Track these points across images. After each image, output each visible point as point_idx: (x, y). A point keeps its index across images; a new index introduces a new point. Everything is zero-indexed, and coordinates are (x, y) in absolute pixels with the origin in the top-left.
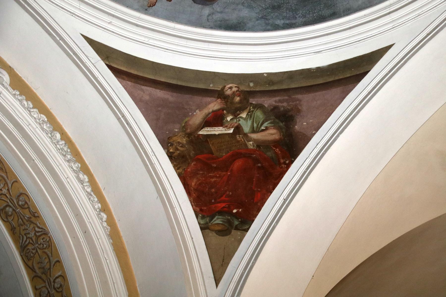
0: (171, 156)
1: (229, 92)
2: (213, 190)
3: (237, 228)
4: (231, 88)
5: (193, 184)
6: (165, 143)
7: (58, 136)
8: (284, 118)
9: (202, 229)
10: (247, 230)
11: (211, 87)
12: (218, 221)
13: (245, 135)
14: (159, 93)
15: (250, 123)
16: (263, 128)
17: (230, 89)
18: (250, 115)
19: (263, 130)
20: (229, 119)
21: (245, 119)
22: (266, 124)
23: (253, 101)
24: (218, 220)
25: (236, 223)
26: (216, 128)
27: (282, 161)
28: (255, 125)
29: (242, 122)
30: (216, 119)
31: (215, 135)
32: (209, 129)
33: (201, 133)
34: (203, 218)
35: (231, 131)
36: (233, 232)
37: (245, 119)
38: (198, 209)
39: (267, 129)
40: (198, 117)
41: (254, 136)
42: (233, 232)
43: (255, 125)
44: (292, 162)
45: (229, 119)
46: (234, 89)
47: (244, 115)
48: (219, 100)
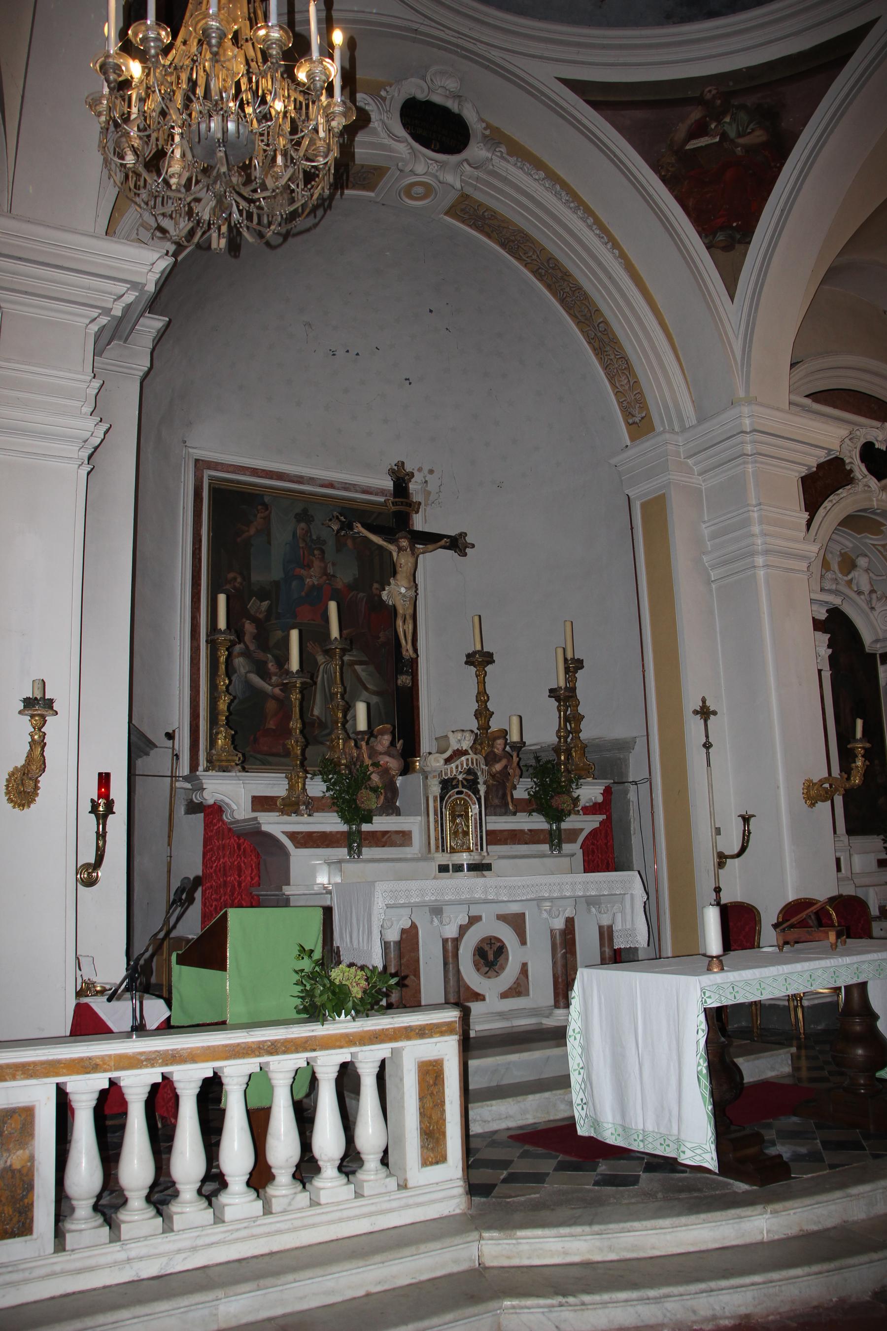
0: (664, 180)
1: (708, 96)
2: (710, 206)
3: (739, 242)
4: (710, 91)
5: (690, 204)
6: (656, 167)
7: (558, 187)
8: (768, 116)
9: (708, 248)
10: (749, 243)
11: (690, 94)
12: (721, 238)
13: (732, 141)
14: (639, 114)
15: (734, 126)
16: (749, 130)
17: (710, 92)
18: (733, 119)
19: (749, 133)
20: (713, 126)
21: (730, 124)
22: (751, 126)
23: (735, 102)
24: (720, 237)
25: (738, 236)
26: (702, 139)
27: (773, 164)
28: (741, 129)
29: (727, 128)
30: (699, 130)
31: (702, 147)
32: (694, 141)
33: (687, 147)
34: (706, 236)
35: (717, 140)
36: (737, 246)
37: (730, 124)
38: (700, 229)
39: (753, 130)
40: (682, 130)
41: (741, 141)
42: (737, 246)
43: (741, 129)
44: (783, 165)
45: (713, 126)
46: (714, 92)
47: (727, 119)
48: (700, 108)
